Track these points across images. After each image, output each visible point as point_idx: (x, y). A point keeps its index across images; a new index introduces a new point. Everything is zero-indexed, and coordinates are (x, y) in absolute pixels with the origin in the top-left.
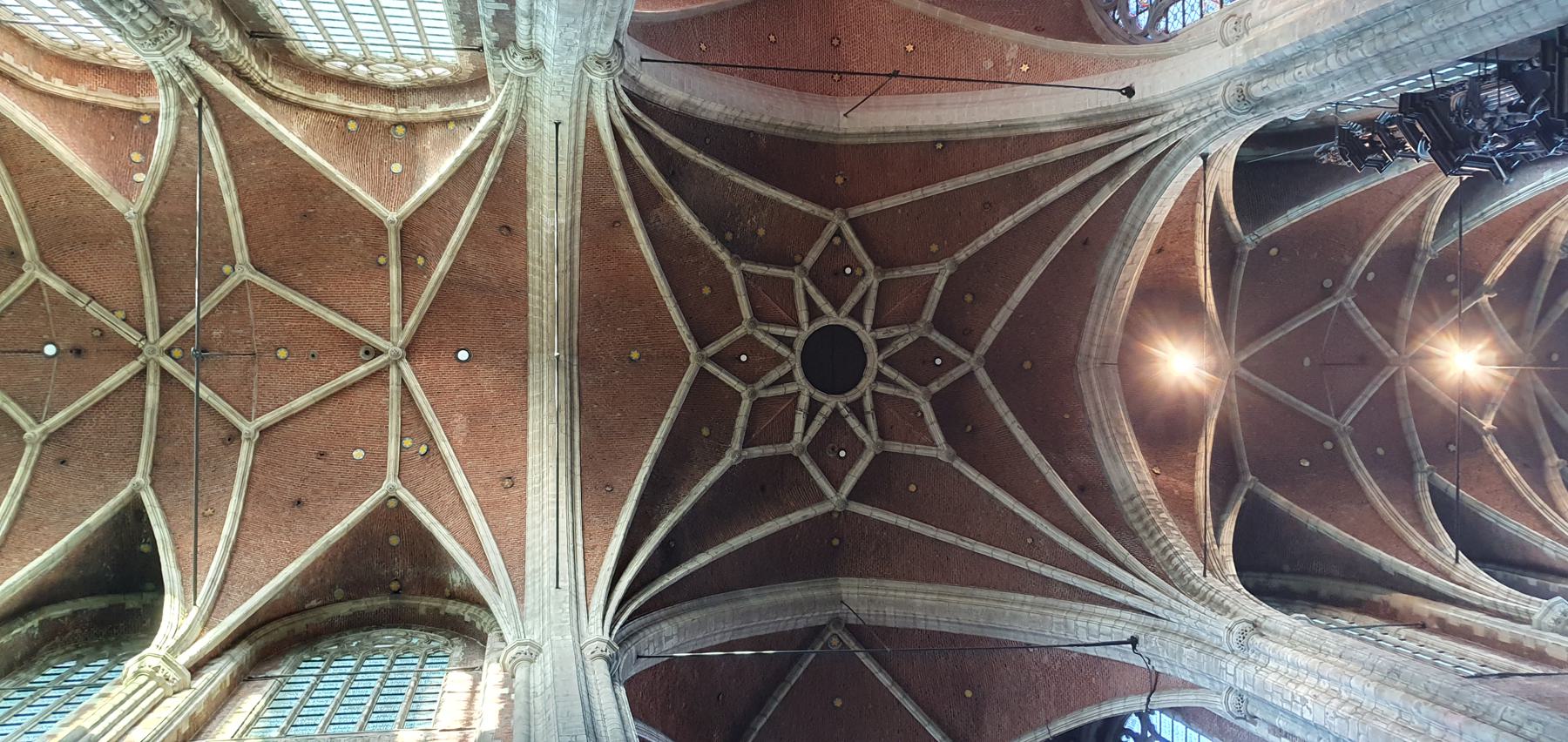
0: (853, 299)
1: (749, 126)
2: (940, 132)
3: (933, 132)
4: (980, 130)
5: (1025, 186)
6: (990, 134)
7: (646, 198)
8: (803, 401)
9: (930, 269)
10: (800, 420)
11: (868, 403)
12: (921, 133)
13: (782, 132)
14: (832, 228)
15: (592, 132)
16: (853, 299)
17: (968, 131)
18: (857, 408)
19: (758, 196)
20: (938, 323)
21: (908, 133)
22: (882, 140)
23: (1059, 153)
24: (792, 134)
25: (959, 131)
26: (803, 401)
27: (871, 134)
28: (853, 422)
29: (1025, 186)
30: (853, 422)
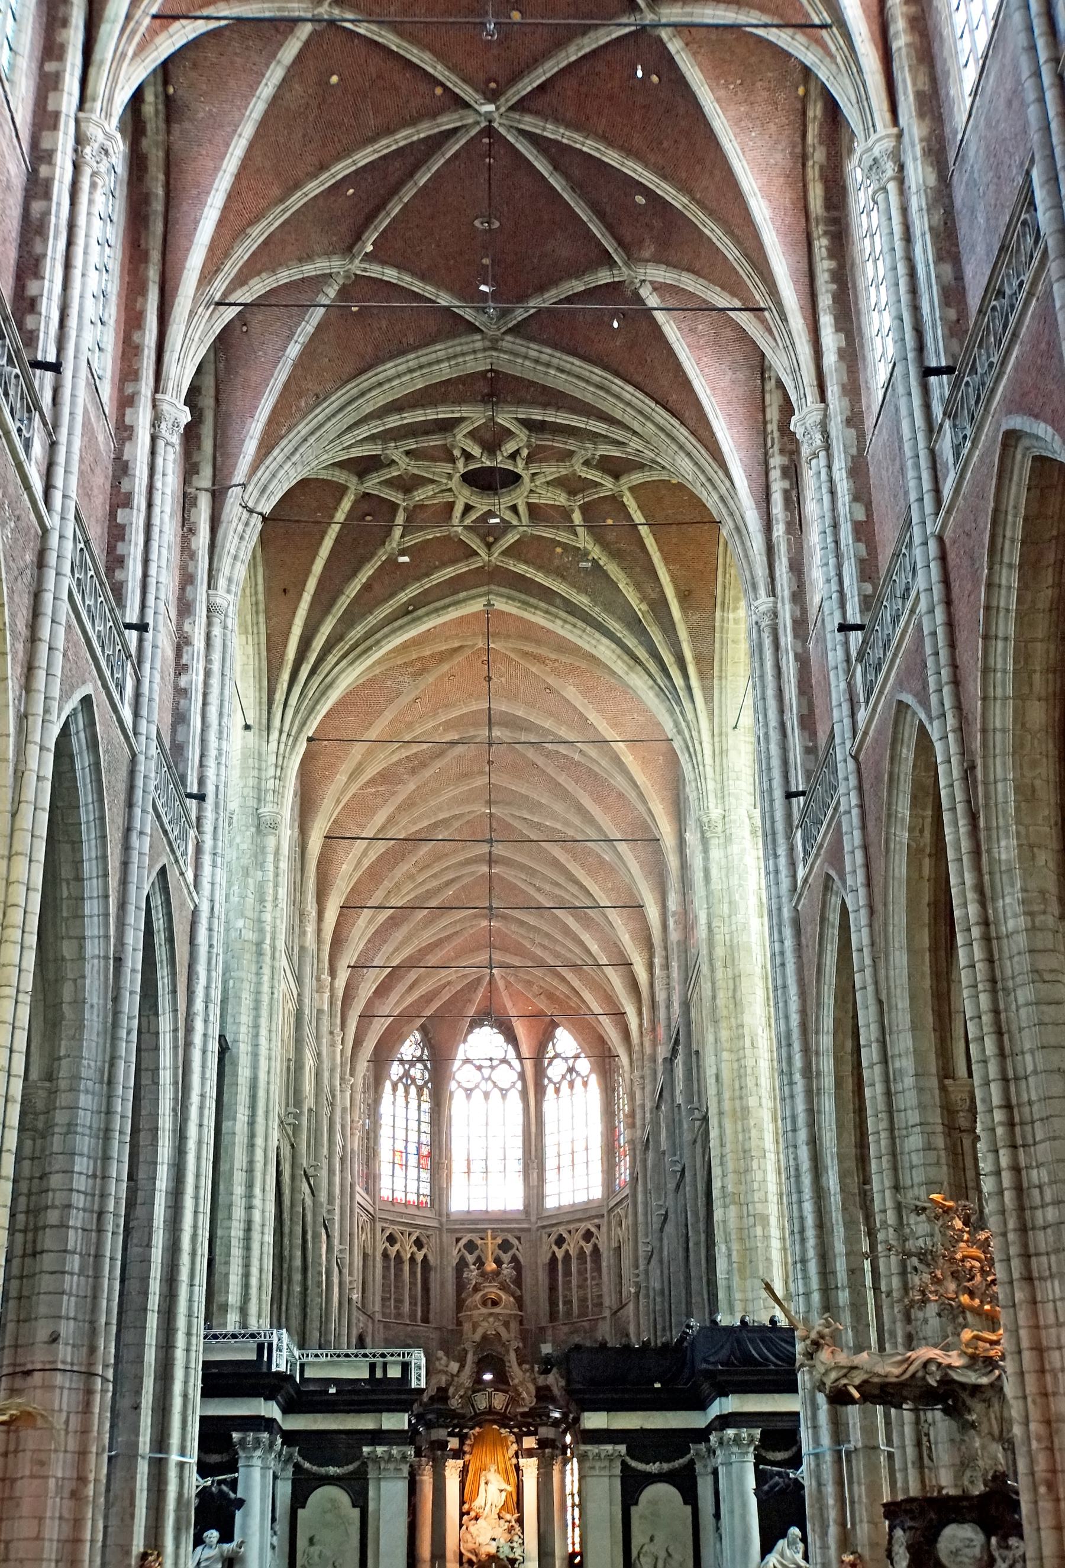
0: (473, 516)
1: (570, 618)
2: (414, 620)
3: (419, 618)
4: (386, 636)
5: (348, 620)
6: (378, 636)
7: (659, 607)
8: (521, 464)
9: (410, 541)
10: (525, 453)
11: (460, 463)
12: (427, 614)
13: (542, 605)
14: (497, 550)
15: (709, 699)
16: (473, 516)
17: (394, 631)
18: (468, 456)
19: (564, 578)
20: (394, 507)
21: (437, 610)
22: (456, 598)
23: (332, 659)
24: (533, 601)
25: (401, 627)
26: (521, 464)
27: (465, 600)
28: (476, 451)
29: (348, 620)
30: (476, 451)
